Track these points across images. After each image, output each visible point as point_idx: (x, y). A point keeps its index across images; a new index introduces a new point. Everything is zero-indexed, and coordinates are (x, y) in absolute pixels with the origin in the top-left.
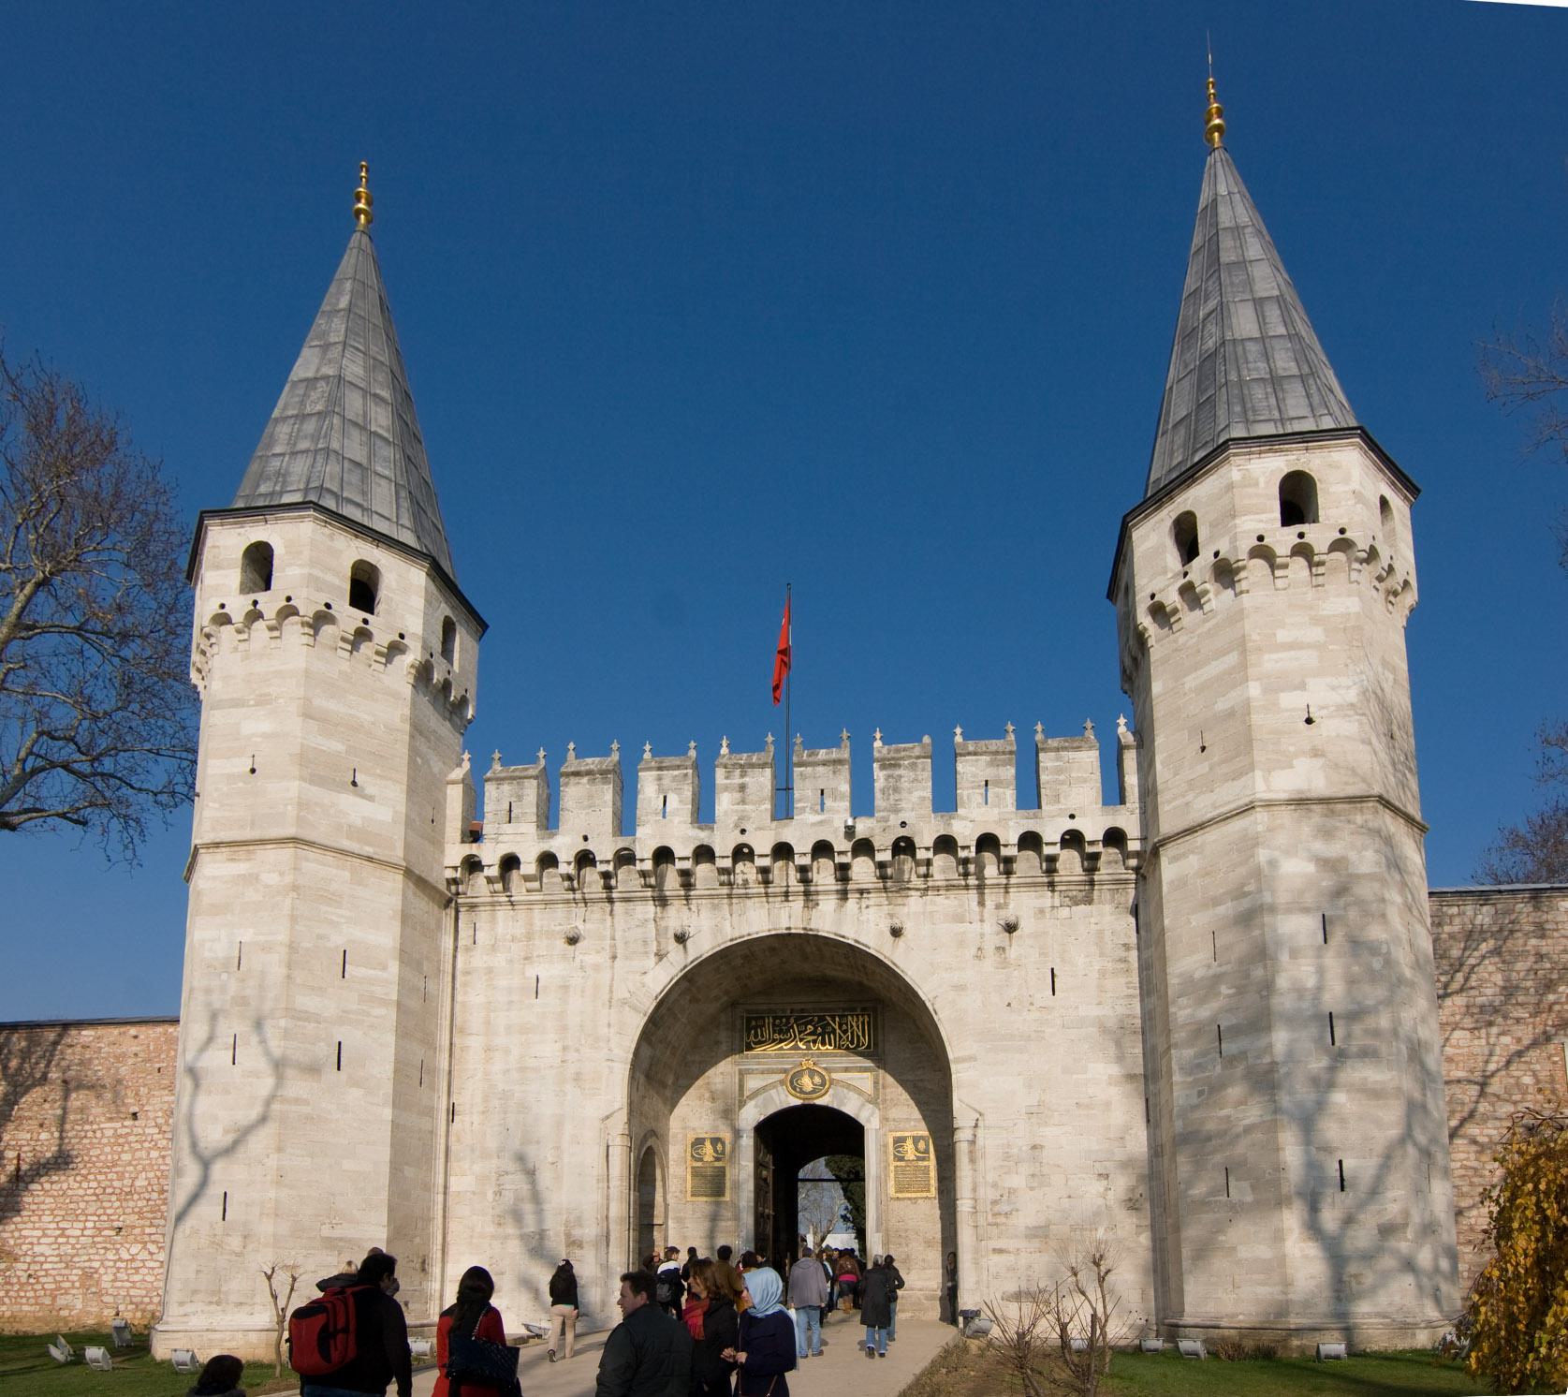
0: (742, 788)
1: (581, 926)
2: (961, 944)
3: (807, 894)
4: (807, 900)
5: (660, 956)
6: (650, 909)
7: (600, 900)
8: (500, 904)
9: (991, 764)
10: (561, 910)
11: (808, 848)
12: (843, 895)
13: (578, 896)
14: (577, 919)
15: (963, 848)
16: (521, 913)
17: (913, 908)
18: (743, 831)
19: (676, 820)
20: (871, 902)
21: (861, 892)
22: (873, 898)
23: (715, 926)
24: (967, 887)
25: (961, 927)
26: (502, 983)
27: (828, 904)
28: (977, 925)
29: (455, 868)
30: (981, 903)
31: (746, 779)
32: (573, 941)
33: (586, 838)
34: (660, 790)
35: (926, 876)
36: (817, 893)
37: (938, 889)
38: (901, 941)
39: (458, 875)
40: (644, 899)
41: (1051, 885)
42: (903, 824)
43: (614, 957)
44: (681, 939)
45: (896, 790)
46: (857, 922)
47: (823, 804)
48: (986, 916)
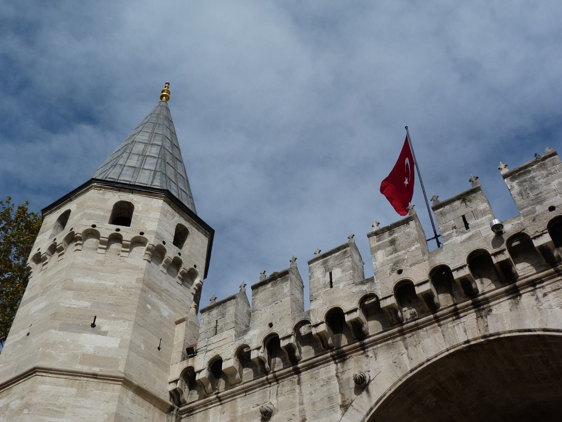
0: (393, 242)
1: (274, 402)
5: (345, 407)
6: (332, 367)
8: (211, 403)
11: (463, 261)
12: (514, 293)
13: (270, 376)
18: (400, 272)
19: (341, 285)
20: (548, 289)
21: (533, 284)
22: (548, 286)
29: (176, 381)
31: (396, 235)
33: (271, 325)
36: (487, 301)
39: (178, 385)
40: (325, 361)
42: (552, 209)
44: (362, 384)
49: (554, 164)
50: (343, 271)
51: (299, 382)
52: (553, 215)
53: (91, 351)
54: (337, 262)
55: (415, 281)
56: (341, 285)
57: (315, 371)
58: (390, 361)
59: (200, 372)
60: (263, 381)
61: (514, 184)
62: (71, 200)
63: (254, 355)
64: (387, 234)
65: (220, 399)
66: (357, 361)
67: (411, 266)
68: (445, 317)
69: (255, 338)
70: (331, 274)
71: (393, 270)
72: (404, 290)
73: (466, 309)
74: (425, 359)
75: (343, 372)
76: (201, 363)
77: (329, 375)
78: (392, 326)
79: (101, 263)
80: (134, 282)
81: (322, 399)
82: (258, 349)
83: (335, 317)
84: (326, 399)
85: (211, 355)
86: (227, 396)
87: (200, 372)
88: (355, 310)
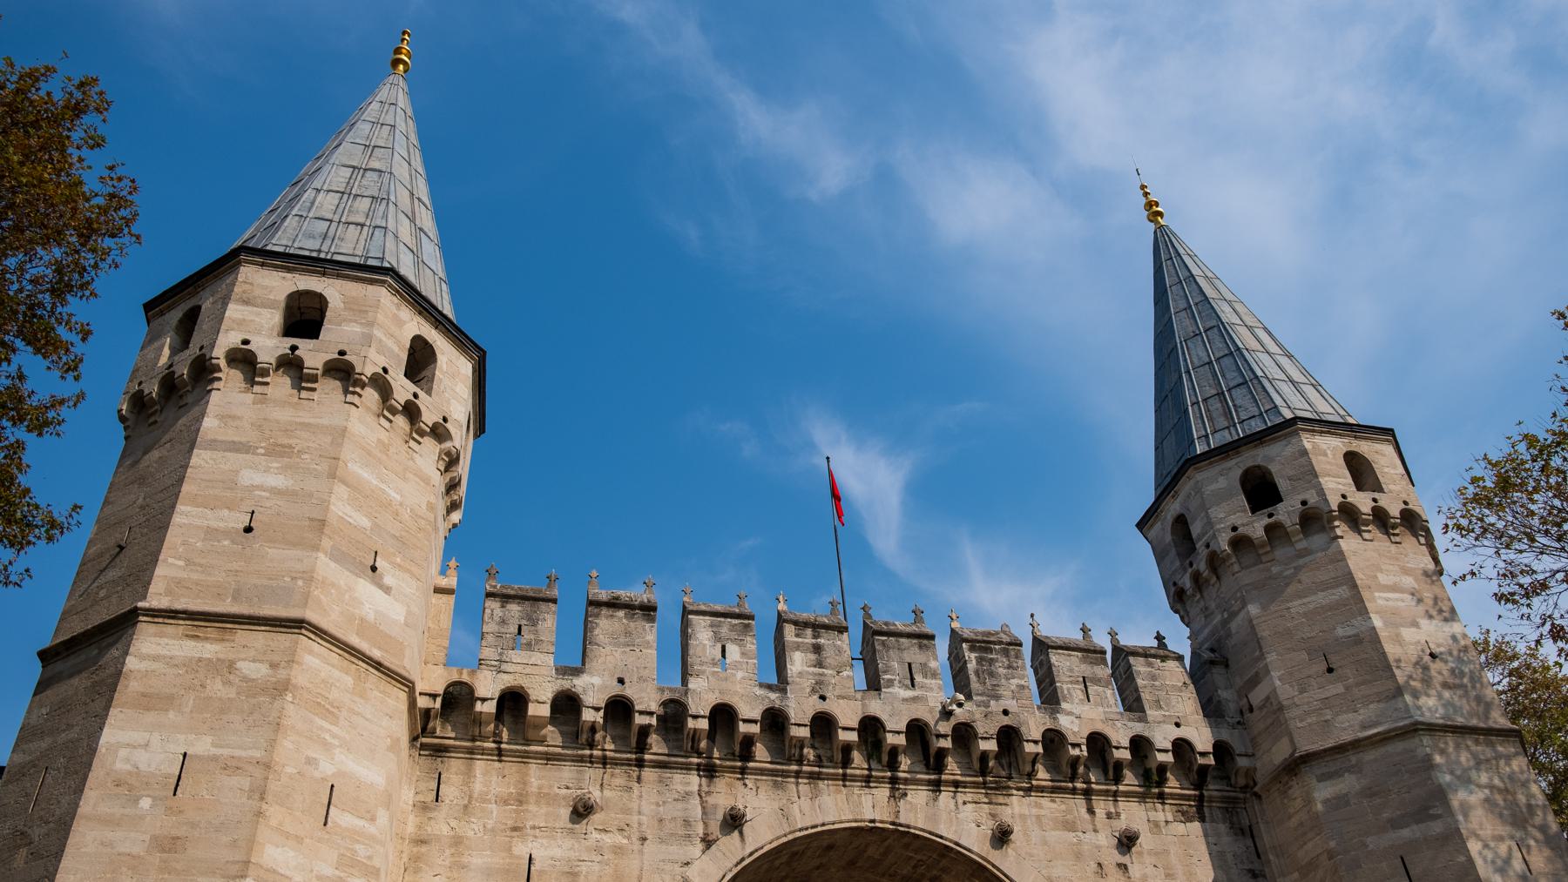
0: (817, 649)
2: (1078, 856)
3: (894, 781)
4: (893, 789)
5: (708, 843)
6: (694, 781)
7: (627, 762)
8: (483, 751)
9: (1084, 660)
10: (567, 772)
12: (936, 786)
13: (595, 752)
14: (589, 782)
15: (1075, 745)
16: (511, 767)
17: (1017, 808)
19: (740, 675)
21: (956, 784)
22: (968, 795)
23: (777, 811)
24: (1074, 791)
25: (1071, 837)
26: (477, 860)
27: (918, 797)
28: (1090, 836)
30: (1091, 811)
31: (822, 641)
32: (582, 811)
33: (621, 681)
34: (717, 637)
35: (1031, 775)
37: (1041, 789)
38: (1010, 850)
40: (687, 768)
41: (1161, 797)
42: (1006, 712)
43: (644, 839)
45: (992, 674)
46: (954, 818)
47: (912, 679)
48: (1099, 826)
49: (1017, 657)
50: (743, 654)
51: (639, 780)
52: (1006, 721)
53: (371, 617)
54: (734, 635)
55: (843, 722)
56: (740, 675)
57: (667, 774)
58: (776, 805)
59: (484, 700)
60: (582, 756)
61: (973, 655)
62: (324, 274)
63: (588, 716)
64: (809, 632)
65: (500, 753)
66: (730, 786)
67: (839, 697)
68: (854, 778)
69: (594, 689)
70: (723, 648)
71: (813, 691)
72: (823, 724)
73: (879, 780)
74: (820, 821)
75: (708, 793)
76: (488, 687)
77: (688, 789)
78: (789, 761)
79: (385, 448)
80: (424, 507)
81: (674, 819)
82: (597, 709)
83: (723, 715)
84: (680, 822)
85: (506, 681)
86: (514, 754)
87: (484, 700)
88: (755, 722)
